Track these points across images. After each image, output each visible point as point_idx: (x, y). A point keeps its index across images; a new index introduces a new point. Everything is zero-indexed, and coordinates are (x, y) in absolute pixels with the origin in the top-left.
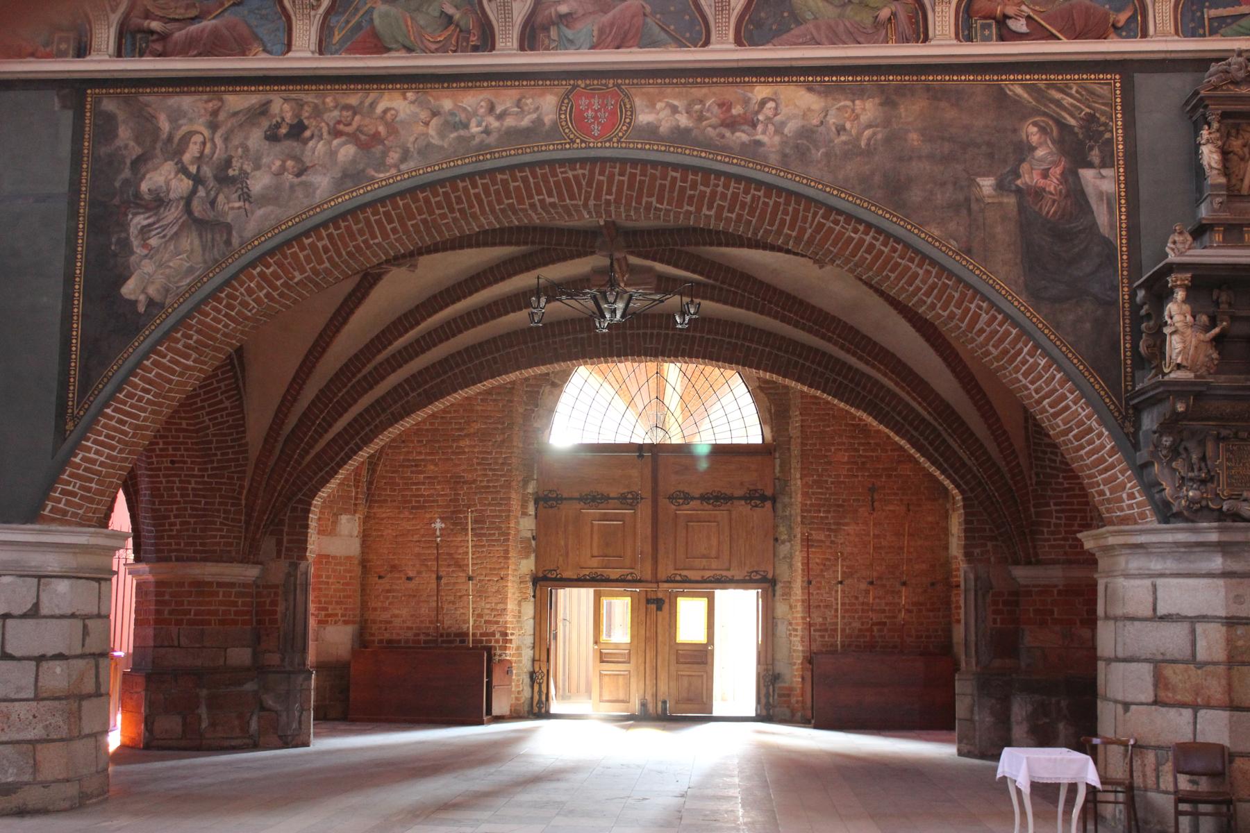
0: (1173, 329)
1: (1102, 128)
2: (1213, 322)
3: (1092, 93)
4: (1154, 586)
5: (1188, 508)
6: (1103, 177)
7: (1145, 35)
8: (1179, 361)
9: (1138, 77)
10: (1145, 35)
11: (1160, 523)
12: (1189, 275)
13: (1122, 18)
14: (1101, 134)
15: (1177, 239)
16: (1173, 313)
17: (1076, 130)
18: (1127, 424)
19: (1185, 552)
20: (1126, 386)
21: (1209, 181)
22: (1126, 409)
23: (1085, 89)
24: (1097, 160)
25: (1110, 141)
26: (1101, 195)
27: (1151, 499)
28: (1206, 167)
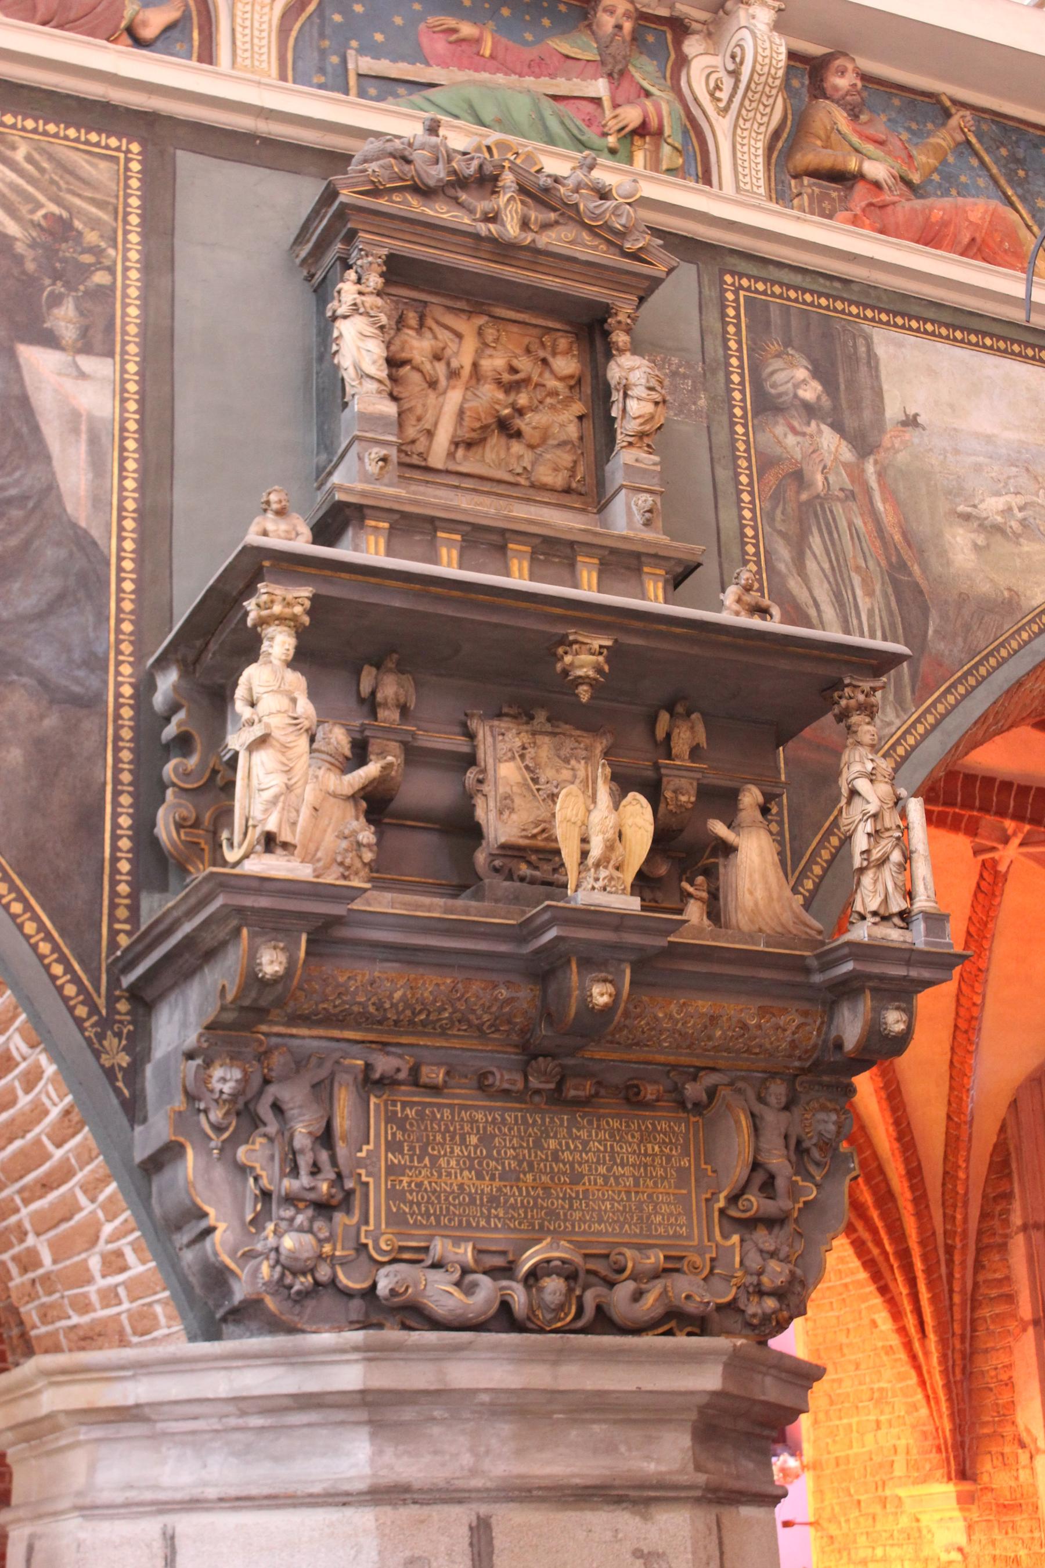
0: (257, 731)
1: (87, 259)
2: (359, 754)
3: (67, 170)
4: (170, 1540)
5: (280, 1286)
6: (82, 375)
7: (207, 55)
8: (271, 826)
9: (186, 161)
10: (207, 55)
11: (192, 1338)
12: (305, 592)
13: (154, 22)
14: (86, 271)
15: (270, 527)
16: (257, 690)
17: (20, 248)
18: (111, 1042)
19: (262, 1429)
20: (113, 934)
21: (356, 406)
22: (112, 1000)
23: (51, 158)
24: (68, 333)
25: (105, 294)
26: (73, 419)
27: (169, 1262)
28: (349, 375)
